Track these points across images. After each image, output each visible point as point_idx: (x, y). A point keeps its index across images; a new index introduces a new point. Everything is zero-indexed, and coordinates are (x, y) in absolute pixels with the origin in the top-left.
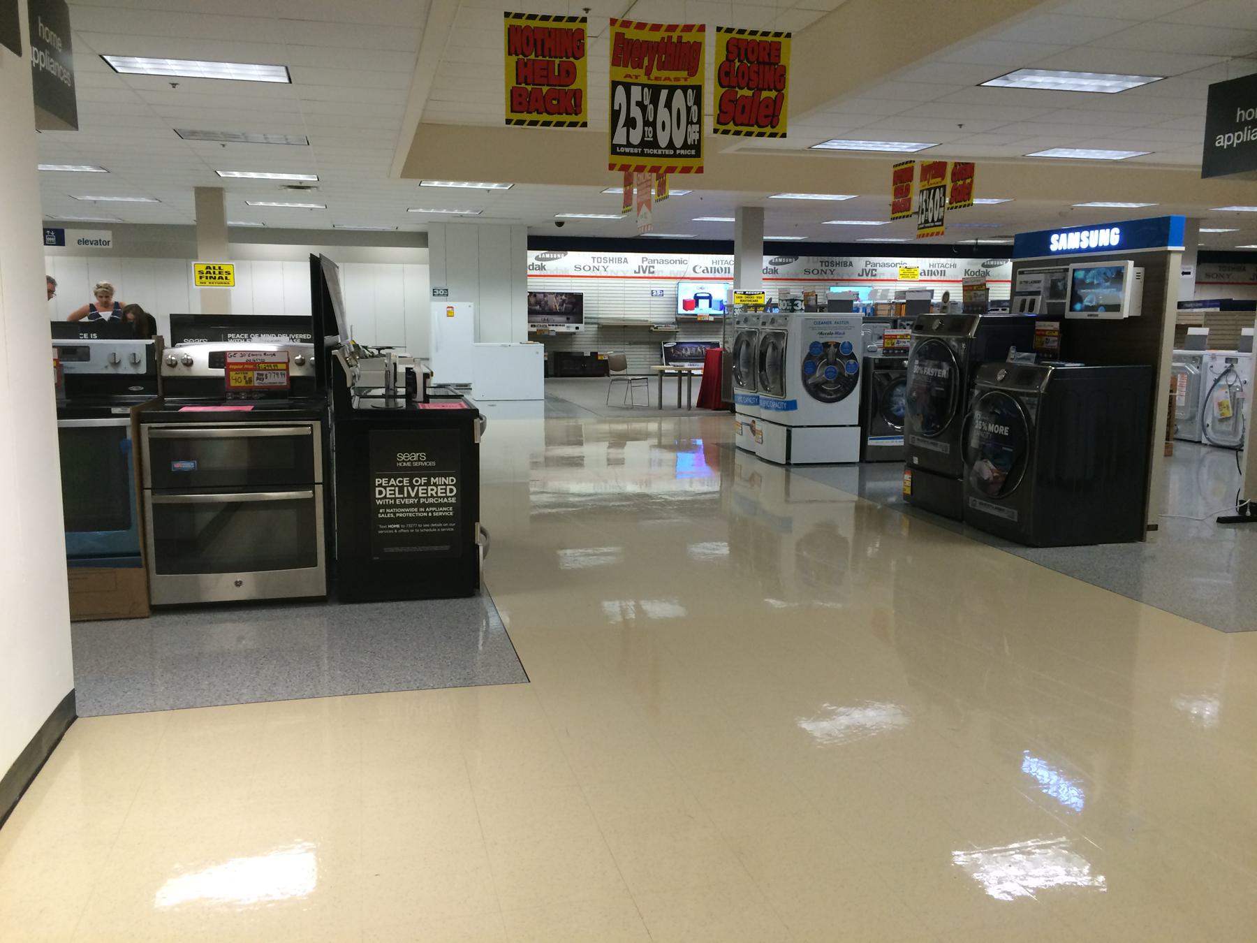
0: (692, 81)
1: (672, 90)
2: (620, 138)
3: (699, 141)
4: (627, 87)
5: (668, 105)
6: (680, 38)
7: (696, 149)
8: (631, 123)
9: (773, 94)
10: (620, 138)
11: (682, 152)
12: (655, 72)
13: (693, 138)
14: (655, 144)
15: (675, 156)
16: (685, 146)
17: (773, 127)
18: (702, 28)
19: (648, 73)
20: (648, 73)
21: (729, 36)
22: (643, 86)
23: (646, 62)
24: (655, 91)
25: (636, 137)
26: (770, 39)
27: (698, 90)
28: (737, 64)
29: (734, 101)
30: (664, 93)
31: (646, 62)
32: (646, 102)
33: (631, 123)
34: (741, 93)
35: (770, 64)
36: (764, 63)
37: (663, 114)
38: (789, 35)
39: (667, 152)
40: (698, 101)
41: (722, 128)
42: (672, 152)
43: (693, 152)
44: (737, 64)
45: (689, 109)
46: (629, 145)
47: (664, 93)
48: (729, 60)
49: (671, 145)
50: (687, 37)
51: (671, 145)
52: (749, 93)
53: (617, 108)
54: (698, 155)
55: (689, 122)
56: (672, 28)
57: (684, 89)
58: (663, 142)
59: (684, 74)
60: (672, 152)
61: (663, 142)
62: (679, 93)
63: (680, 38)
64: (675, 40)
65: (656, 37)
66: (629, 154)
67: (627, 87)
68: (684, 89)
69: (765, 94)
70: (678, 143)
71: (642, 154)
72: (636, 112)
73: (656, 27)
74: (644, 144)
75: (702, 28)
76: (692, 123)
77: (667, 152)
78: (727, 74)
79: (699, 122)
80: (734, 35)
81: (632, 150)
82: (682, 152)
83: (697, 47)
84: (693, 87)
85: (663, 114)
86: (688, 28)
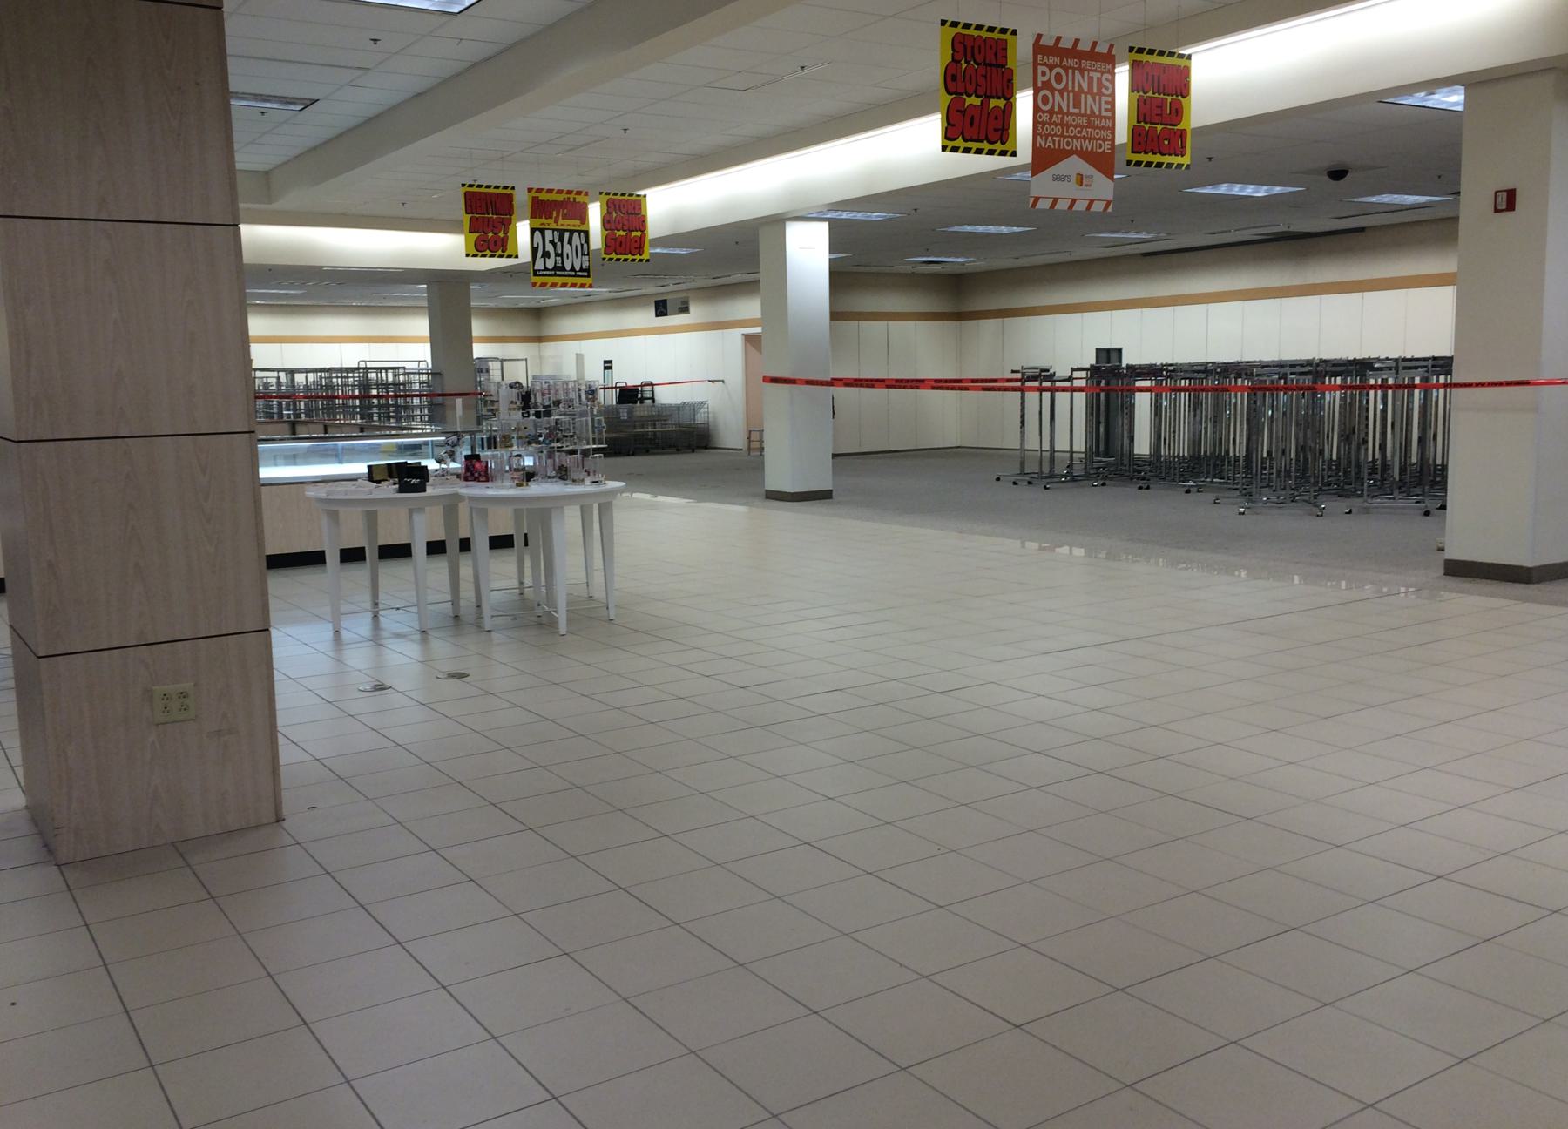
0: (583, 228)
2: (539, 265)
4: (542, 231)
5: (570, 242)
8: (546, 255)
10: (539, 265)
12: (561, 221)
16: (582, 270)
24: (562, 233)
25: (550, 263)
27: (587, 233)
30: (567, 235)
33: (546, 255)
37: (567, 247)
47: (567, 235)
49: (573, 269)
51: (573, 269)
56: (569, 192)
57: (579, 232)
61: (568, 267)
65: (560, 198)
67: (542, 231)
72: (549, 247)
73: (560, 192)
85: (567, 247)
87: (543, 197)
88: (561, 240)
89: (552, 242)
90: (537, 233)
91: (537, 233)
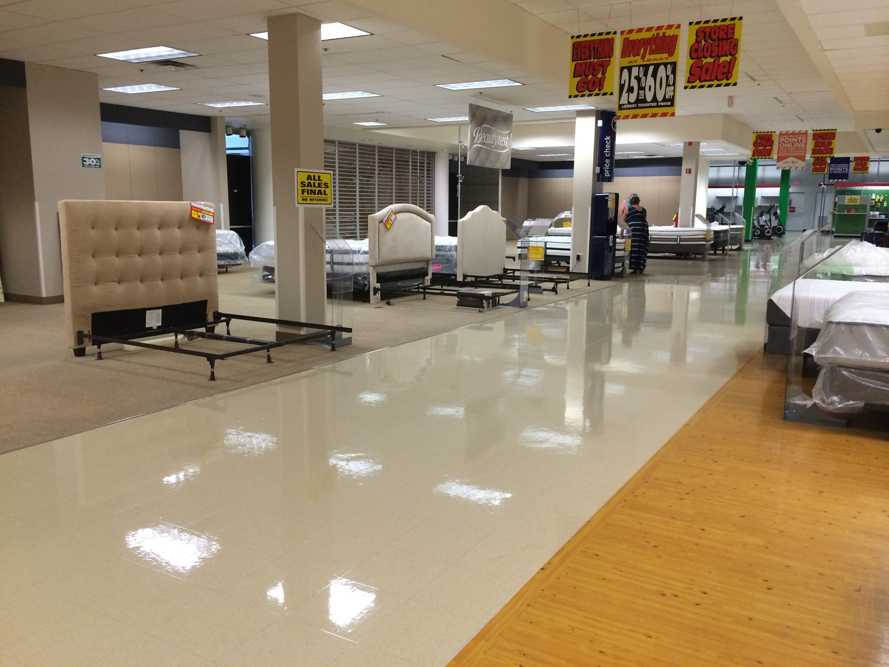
0: (671, 60)
1: (657, 67)
3: (673, 96)
4: (629, 69)
5: (654, 75)
6: (664, 33)
7: (671, 101)
8: (631, 90)
9: (728, 58)
11: (662, 104)
12: (648, 57)
13: (669, 94)
14: (644, 101)
15: (657, 106)
16: (664, 100)
17: (728, 79)
18: (679, 26)
19: (643, 58)
20: (643, 58)
21: (698, 26)
22: (639, 66)
23: (642, 52)
24: (646, 67)
25: (633, 97)
26: (727, 23)
27: (674, 65)
28: (703, 43)
29: (701, 67)
30: (651, 68)
31: (642, 52)
32: (641, 76)
33: (631, 90)
34: (705, 61)
35: (727, 39)
36: (723, 39)
38: (741, 18)
39: (653, 104)
40: (674, 72)
41: (690, 85)
42: (655, 104)
43: (669, 103)
44: (703, 43)
45: (667, 77)
46: (629, 103)
47: (651, 68)
48: (698, 42)
49: (655, 99)
50: (669, 33)
51: (655, 99)
52: (712, 60)
53: (622, 82)
54: (672, 105)
55: (668, 85)
56: (659, 28)
57: (665, 65)
58: (649, 97)
59: (666, 55)
60: (655, 104)
61: (649, 97)
62: (662, 68)
63: (664, 33)
64: (661, 35)
65: (649, 35)
66: (629, 108)
68: (665, 65)
69: (723, 59)
70: (660, 98)
71: (637, 107)
72: (634, 83)
74: (638, 101)
75: (679, 26)
76: (669, 85)
77: (653, 104)
78: (696, 51)
79: (674, 85)
80: (702, 25)
81: (631, 106)
82: (662, 104)
83: (675, 38)
84: (671, 63)
85: (650, 80)
86: (670, 27)
87: (633, 37)
88: (646, 75)
89: (638, 78)
90: (626, 72)
91: (626, 72)
